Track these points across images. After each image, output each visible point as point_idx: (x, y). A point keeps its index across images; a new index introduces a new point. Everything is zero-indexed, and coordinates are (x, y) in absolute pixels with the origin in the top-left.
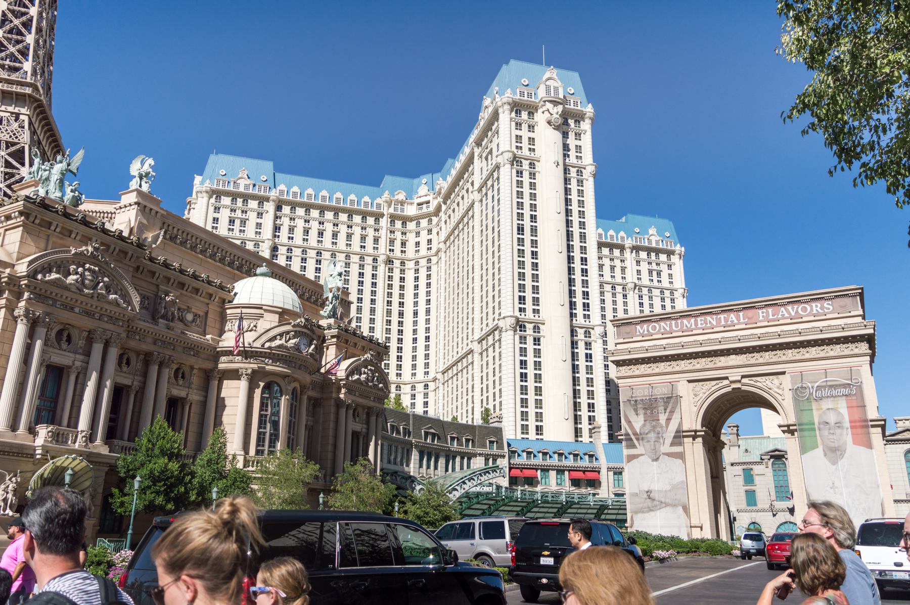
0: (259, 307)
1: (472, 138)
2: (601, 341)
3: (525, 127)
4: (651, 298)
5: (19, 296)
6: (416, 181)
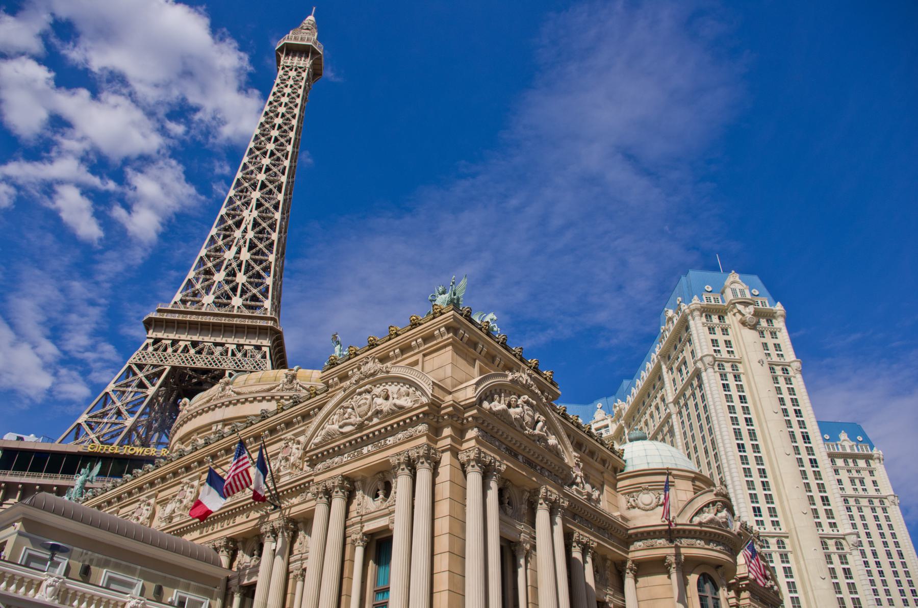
0: (667, 472)
1: (658, 349)
2: (858, 552)
3: (718, 331)
4: (860, 509)
5: (460, 433)
6: (590, 406)
